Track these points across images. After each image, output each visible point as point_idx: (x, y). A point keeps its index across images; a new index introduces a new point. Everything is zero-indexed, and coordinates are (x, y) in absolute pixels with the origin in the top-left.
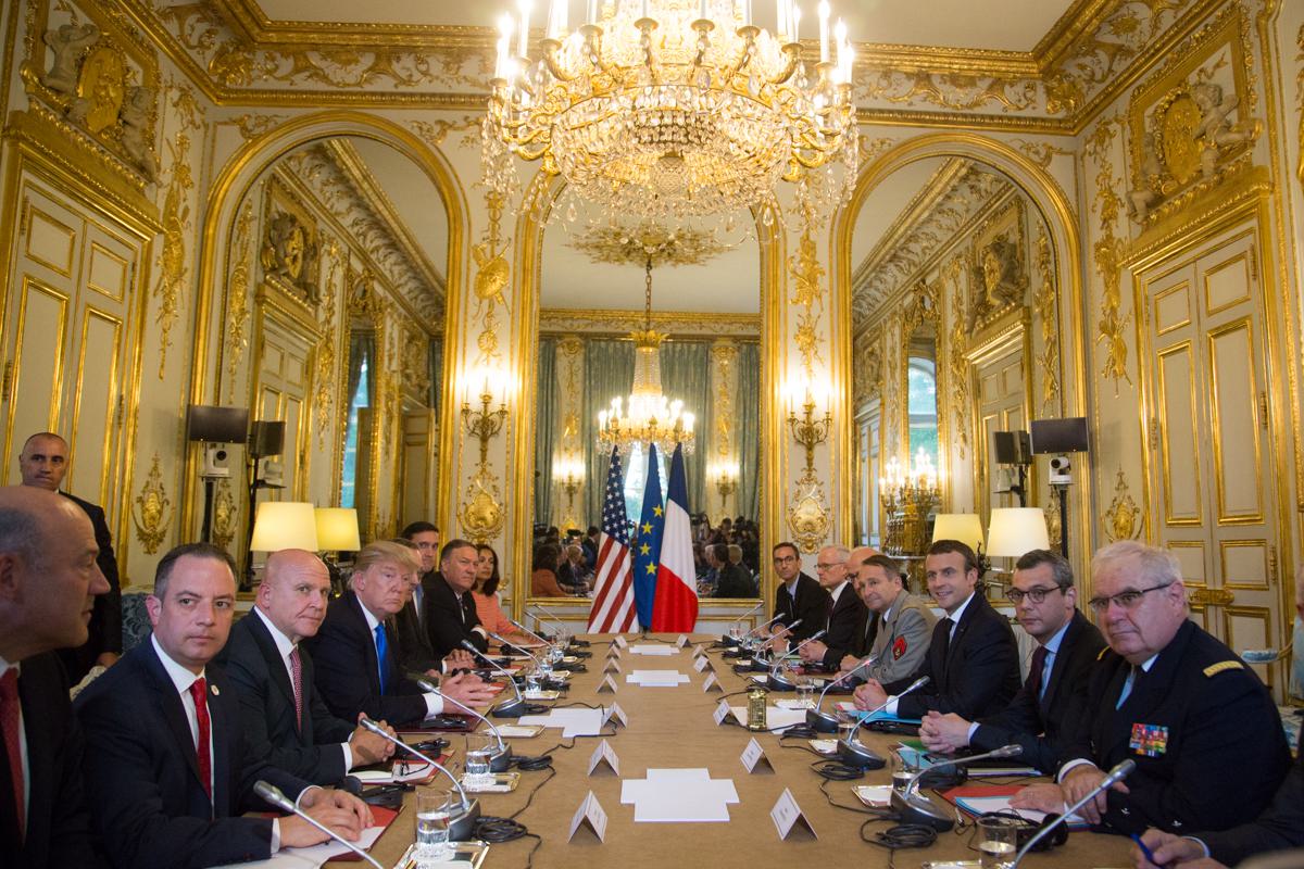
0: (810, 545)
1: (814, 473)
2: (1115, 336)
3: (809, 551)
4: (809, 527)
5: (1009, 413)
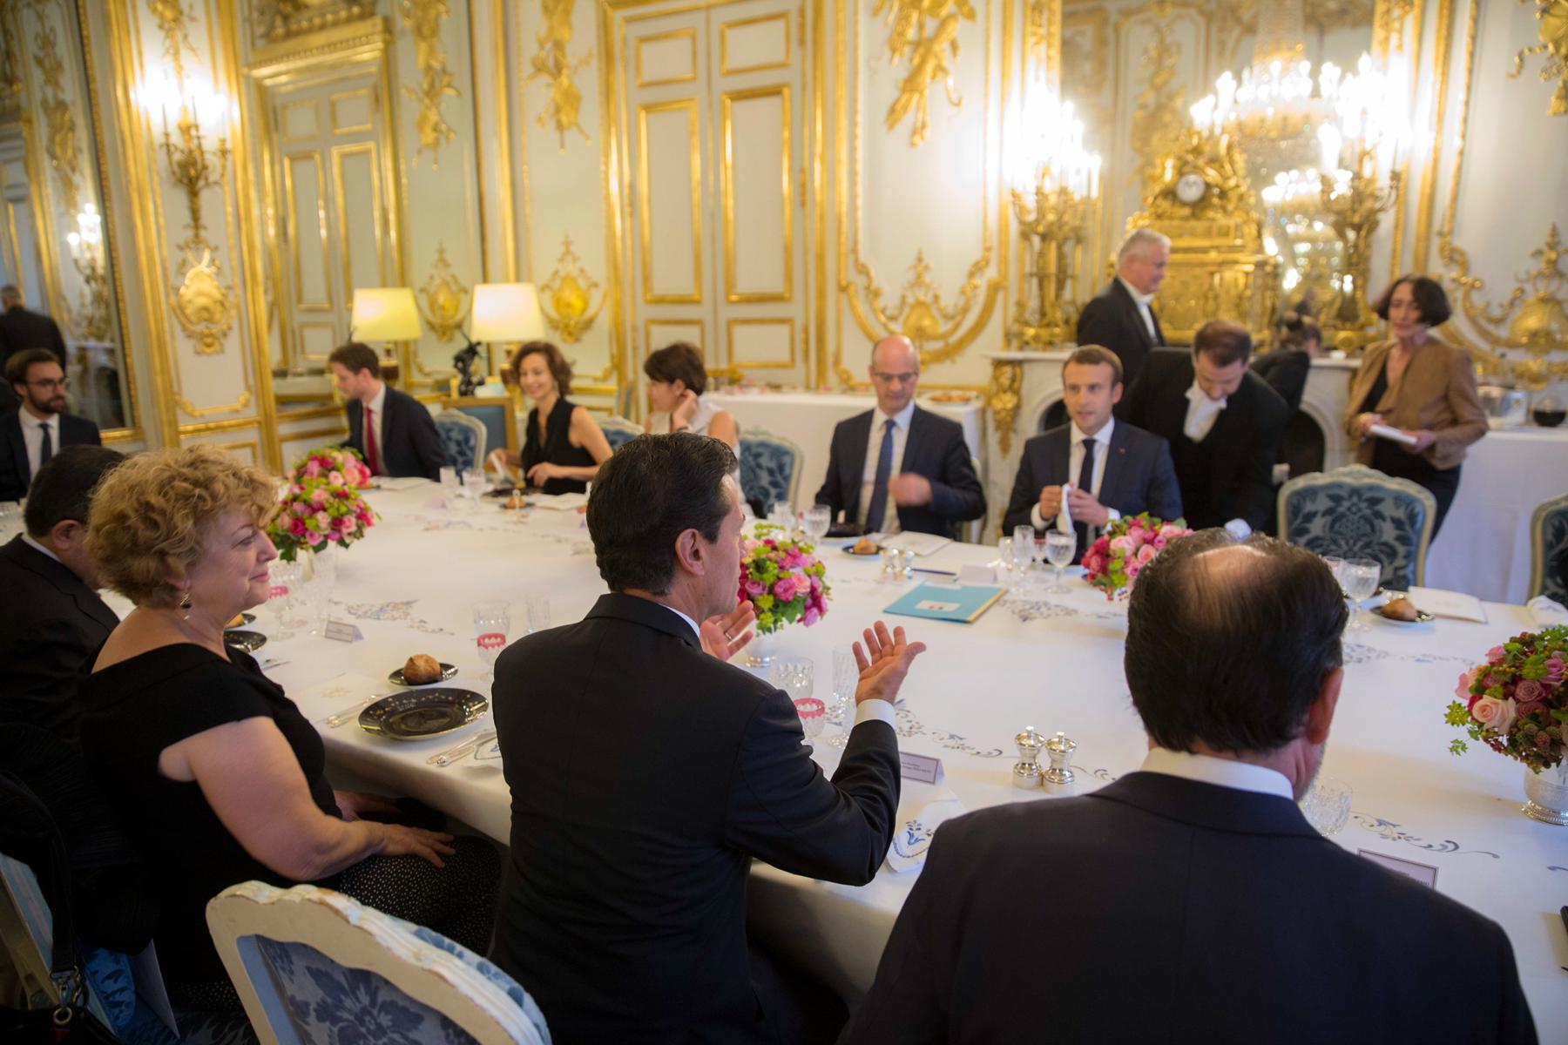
0: (209, 340)
1: (203, 233)
2: (564, 80)
3: (208, 350)
4: (205, 315)
5: (344, 156)
